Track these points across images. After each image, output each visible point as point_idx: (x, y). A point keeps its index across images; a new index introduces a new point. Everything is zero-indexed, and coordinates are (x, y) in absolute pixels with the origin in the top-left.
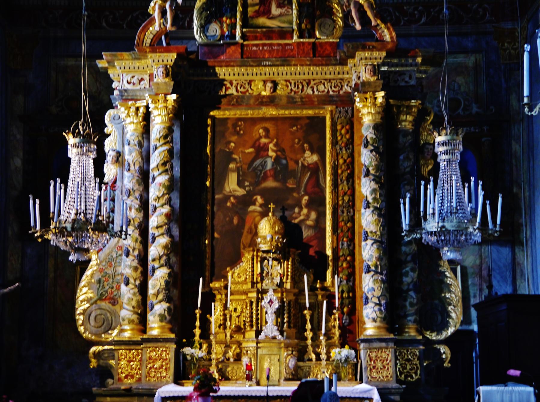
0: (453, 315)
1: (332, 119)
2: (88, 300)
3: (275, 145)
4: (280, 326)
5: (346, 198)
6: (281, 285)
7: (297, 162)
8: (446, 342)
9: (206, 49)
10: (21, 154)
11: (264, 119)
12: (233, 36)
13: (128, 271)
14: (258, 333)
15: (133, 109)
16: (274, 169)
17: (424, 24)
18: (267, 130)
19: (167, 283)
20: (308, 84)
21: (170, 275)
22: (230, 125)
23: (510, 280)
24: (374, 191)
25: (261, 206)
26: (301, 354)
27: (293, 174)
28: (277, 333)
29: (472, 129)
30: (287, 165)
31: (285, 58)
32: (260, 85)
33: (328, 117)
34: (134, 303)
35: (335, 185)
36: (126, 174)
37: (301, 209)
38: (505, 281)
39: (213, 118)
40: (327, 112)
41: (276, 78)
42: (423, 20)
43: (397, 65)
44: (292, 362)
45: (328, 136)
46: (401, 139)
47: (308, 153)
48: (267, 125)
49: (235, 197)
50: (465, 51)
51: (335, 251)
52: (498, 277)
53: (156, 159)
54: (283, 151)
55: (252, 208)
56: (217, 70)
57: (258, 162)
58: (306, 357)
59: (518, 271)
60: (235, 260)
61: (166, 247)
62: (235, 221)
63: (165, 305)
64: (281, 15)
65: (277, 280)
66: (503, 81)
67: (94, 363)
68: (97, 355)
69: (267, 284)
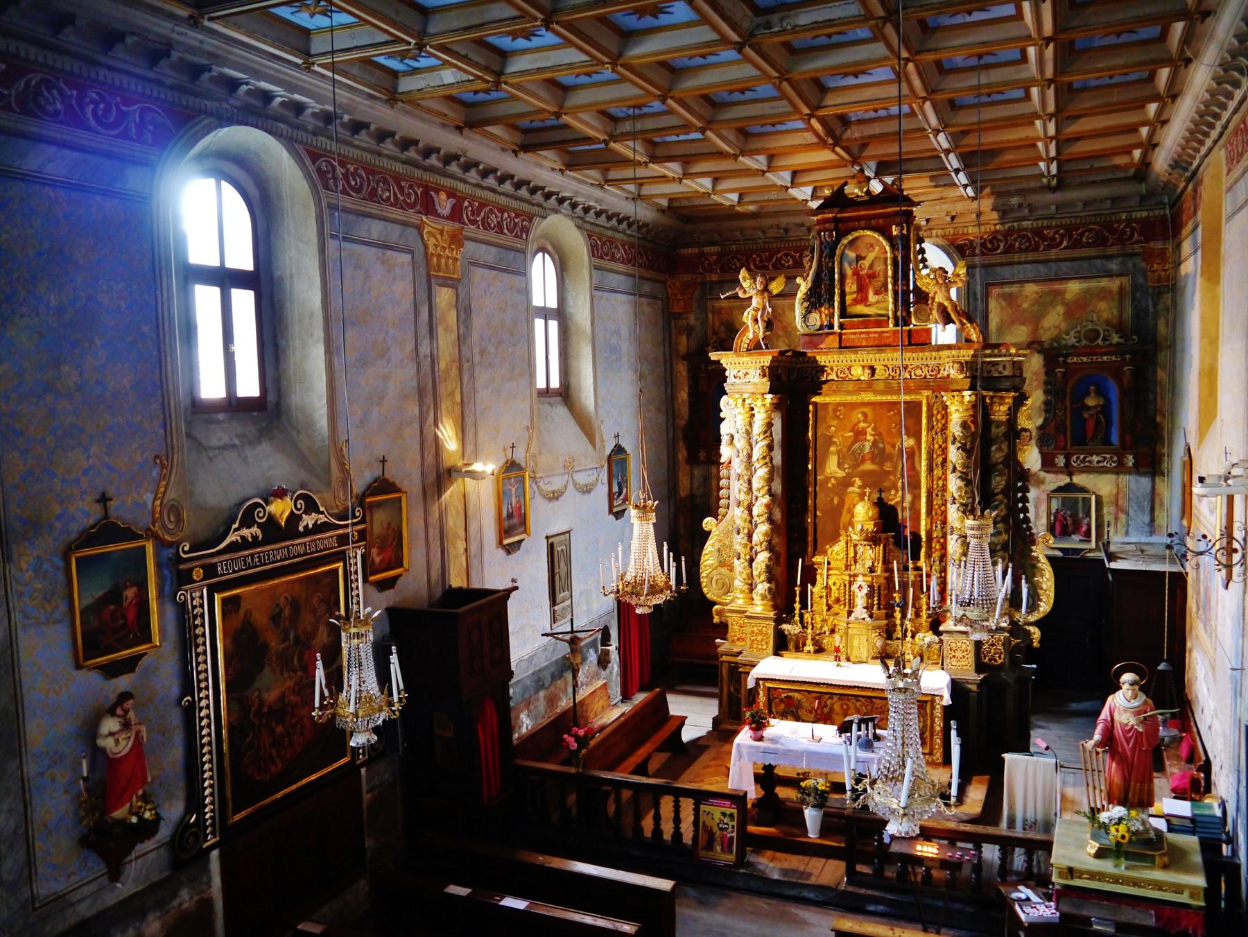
0: (1044, 598)
1: (928, 404)
2: (710, 566)
3: (874, 429)
4: (868, 608)
5: (941, 483)
6: (872, 570)
7: (894, 446)
8: (1036, 624)
9: (806, 338)
10: (686, 388)
11: (863, 404)
12: (831, 326)
13: (738, 548)
14: (850, 613)
15: (740, 401)
16: (872, 452)
17: (1065, 248)
18: (865, 415)
19: (767, 566)
20: (906, 368)
21: (770, 559)
22: (830, 409)
23: (1148, 510)
24: (960, 488)
25: (859, 487)
26: (889, 633)
27: (889, 457)
28: (866, 616)
29: (1114, 358)
30: (883, 450)
31: (880, 346)
32: (860, 370)
33: (924, 402)
34: (744, 576)
35: (930, 470)
36: (737, 460)
37: (897, 491)
38: (1142, 509)
39: (815, 404)
40: (923, 397)
41: (873, 363)
42: (1065, 243)
43: (990, 356)
44: (879, 643)
45: (924, 421)
46: (994, 430)
47: (904, 437)
48: (866, 410)
49: (836, 478)
50: (1109, 275)
51: (929, 533)
52: (1135, 507)
53: (758, 452)
54: (880, 435)
55: (851, 489)
56: (818, 358)
57: (856, 446)
58: (895, 636)
59: (1157, 501)
60: (834, 539)
61: (766, 534)
62: (836, 501)
63: (767, 585)
64: (877, 302)
65: (869, 564)
66: (1150, 304)
67: (716, 619)
68: (720, 613)
69: (858, 568)
